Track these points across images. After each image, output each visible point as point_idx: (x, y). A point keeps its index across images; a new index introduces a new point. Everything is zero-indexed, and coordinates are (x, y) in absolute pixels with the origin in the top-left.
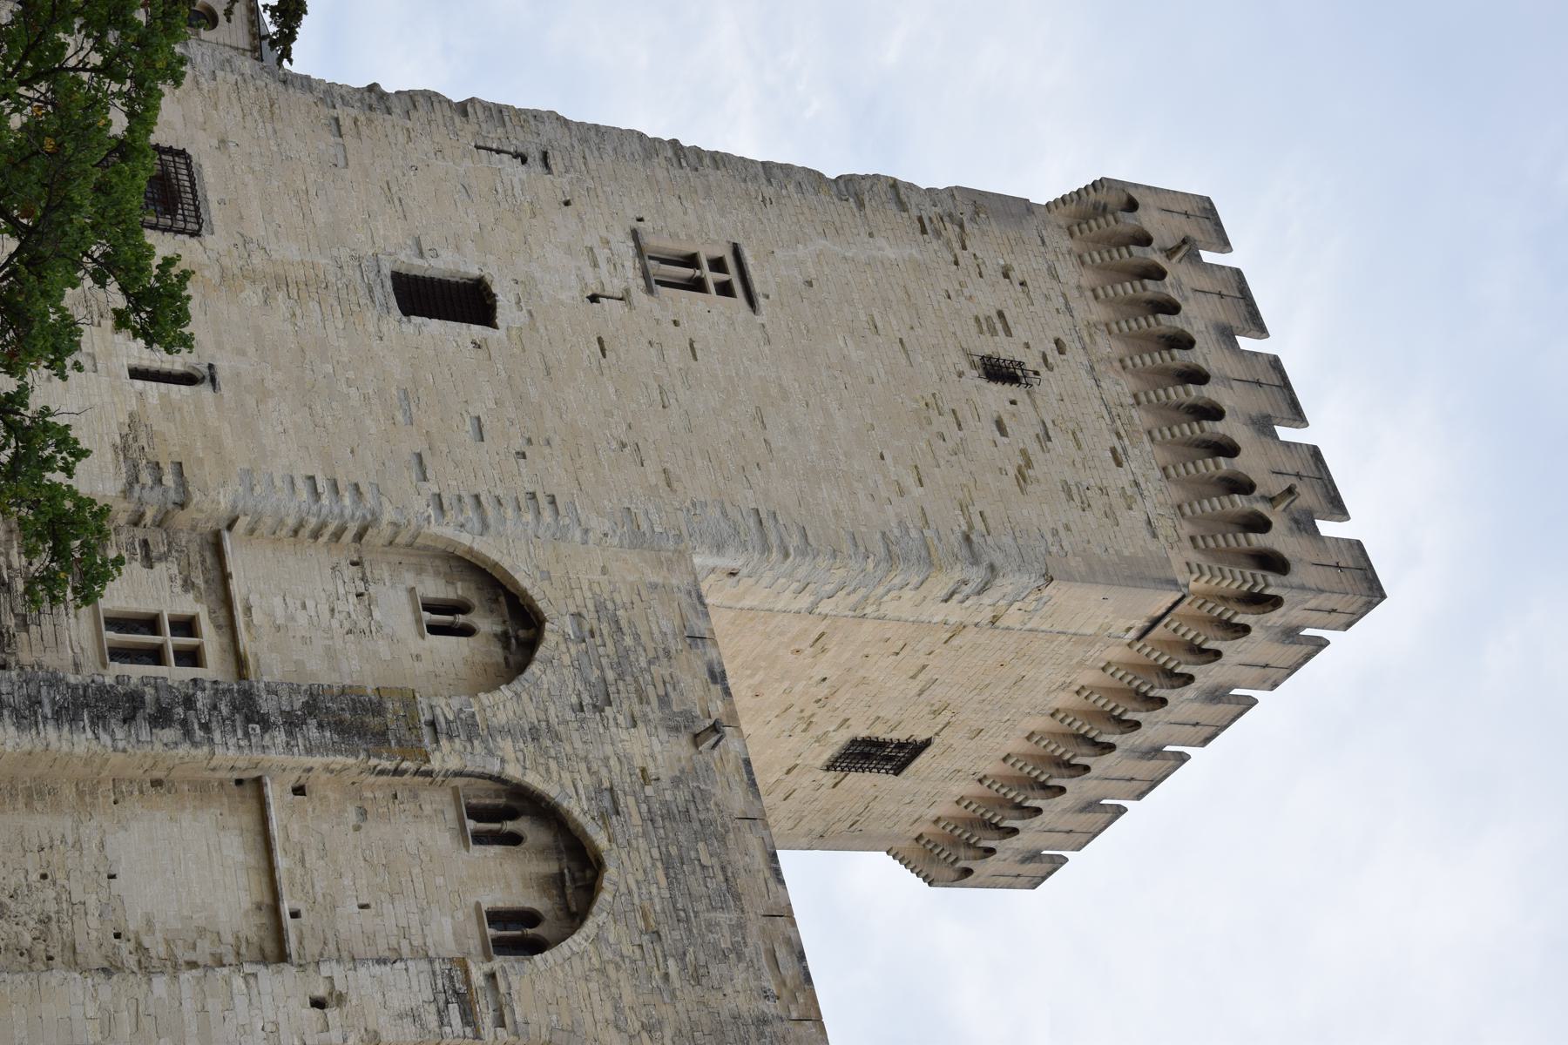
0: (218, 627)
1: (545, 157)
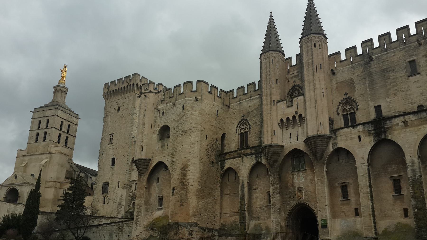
0: (136, 181)
1: (102, 152)
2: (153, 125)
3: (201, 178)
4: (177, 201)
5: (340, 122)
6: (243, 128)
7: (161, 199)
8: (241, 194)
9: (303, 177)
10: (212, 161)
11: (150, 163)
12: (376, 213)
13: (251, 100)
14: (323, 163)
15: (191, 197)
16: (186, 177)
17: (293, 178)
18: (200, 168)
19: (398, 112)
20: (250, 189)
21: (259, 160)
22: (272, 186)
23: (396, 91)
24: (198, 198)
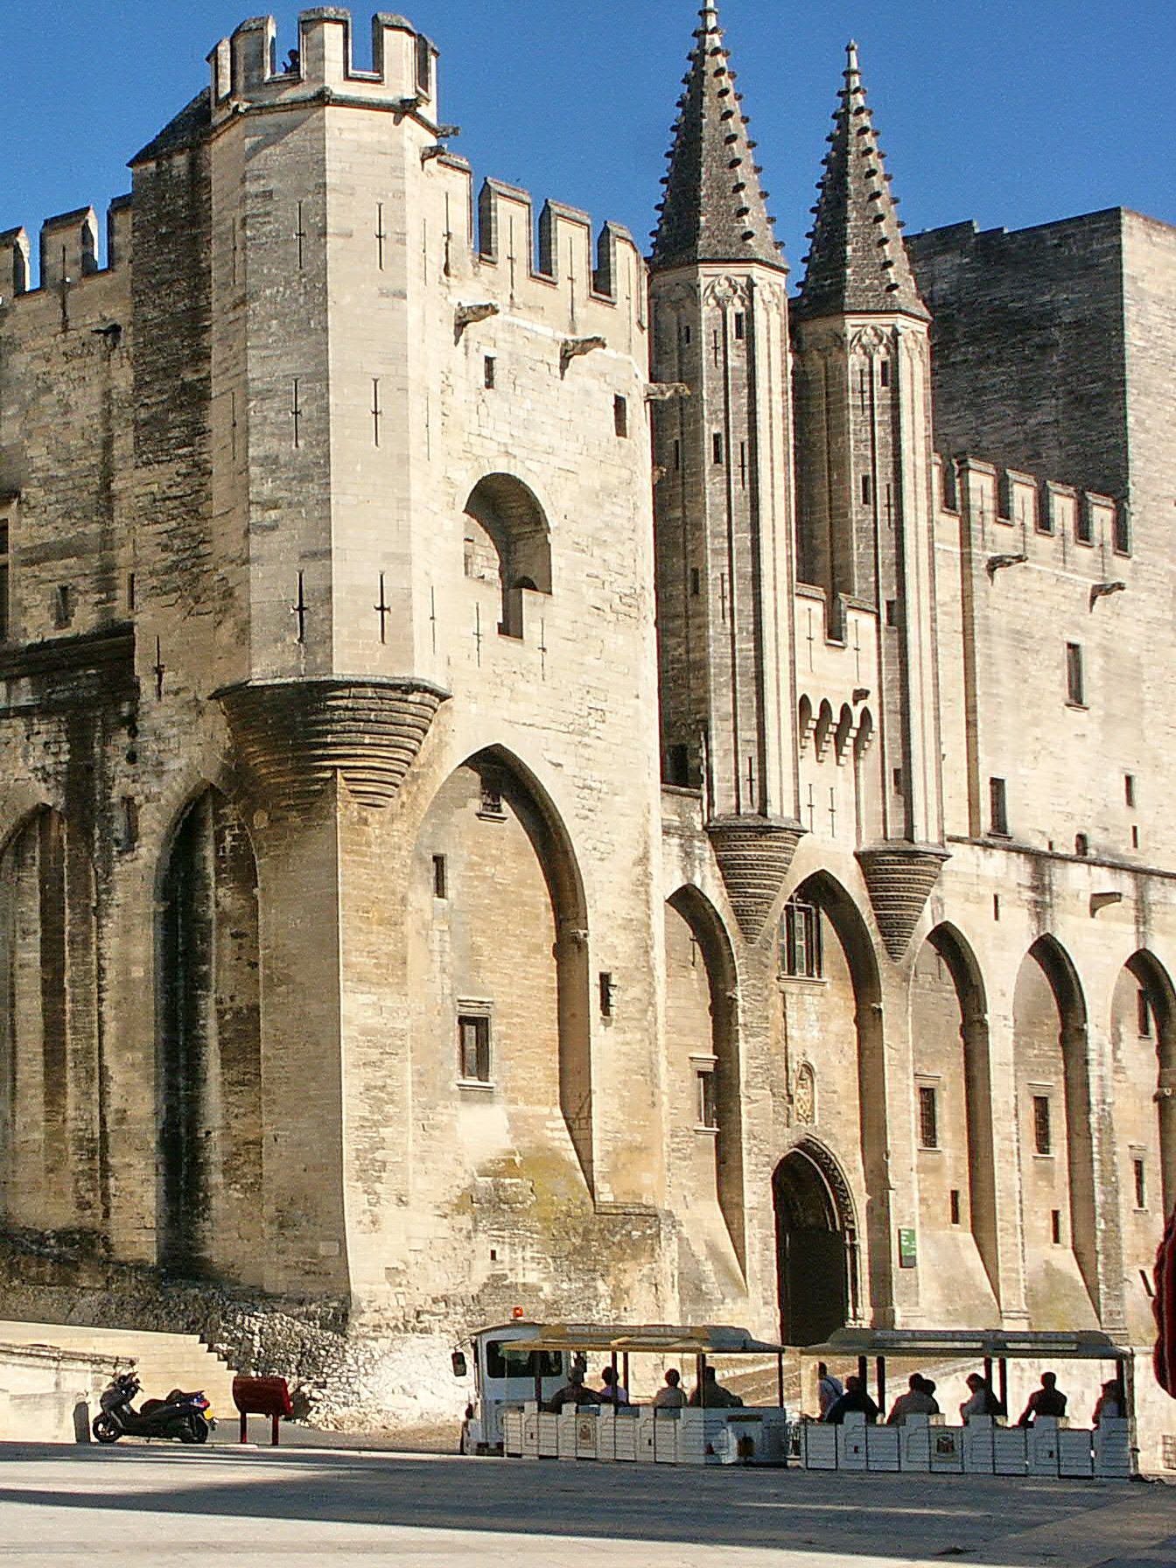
7: (475, 1026)
9: (813, 1017)
11: (431, 729)
14: (906, 980)
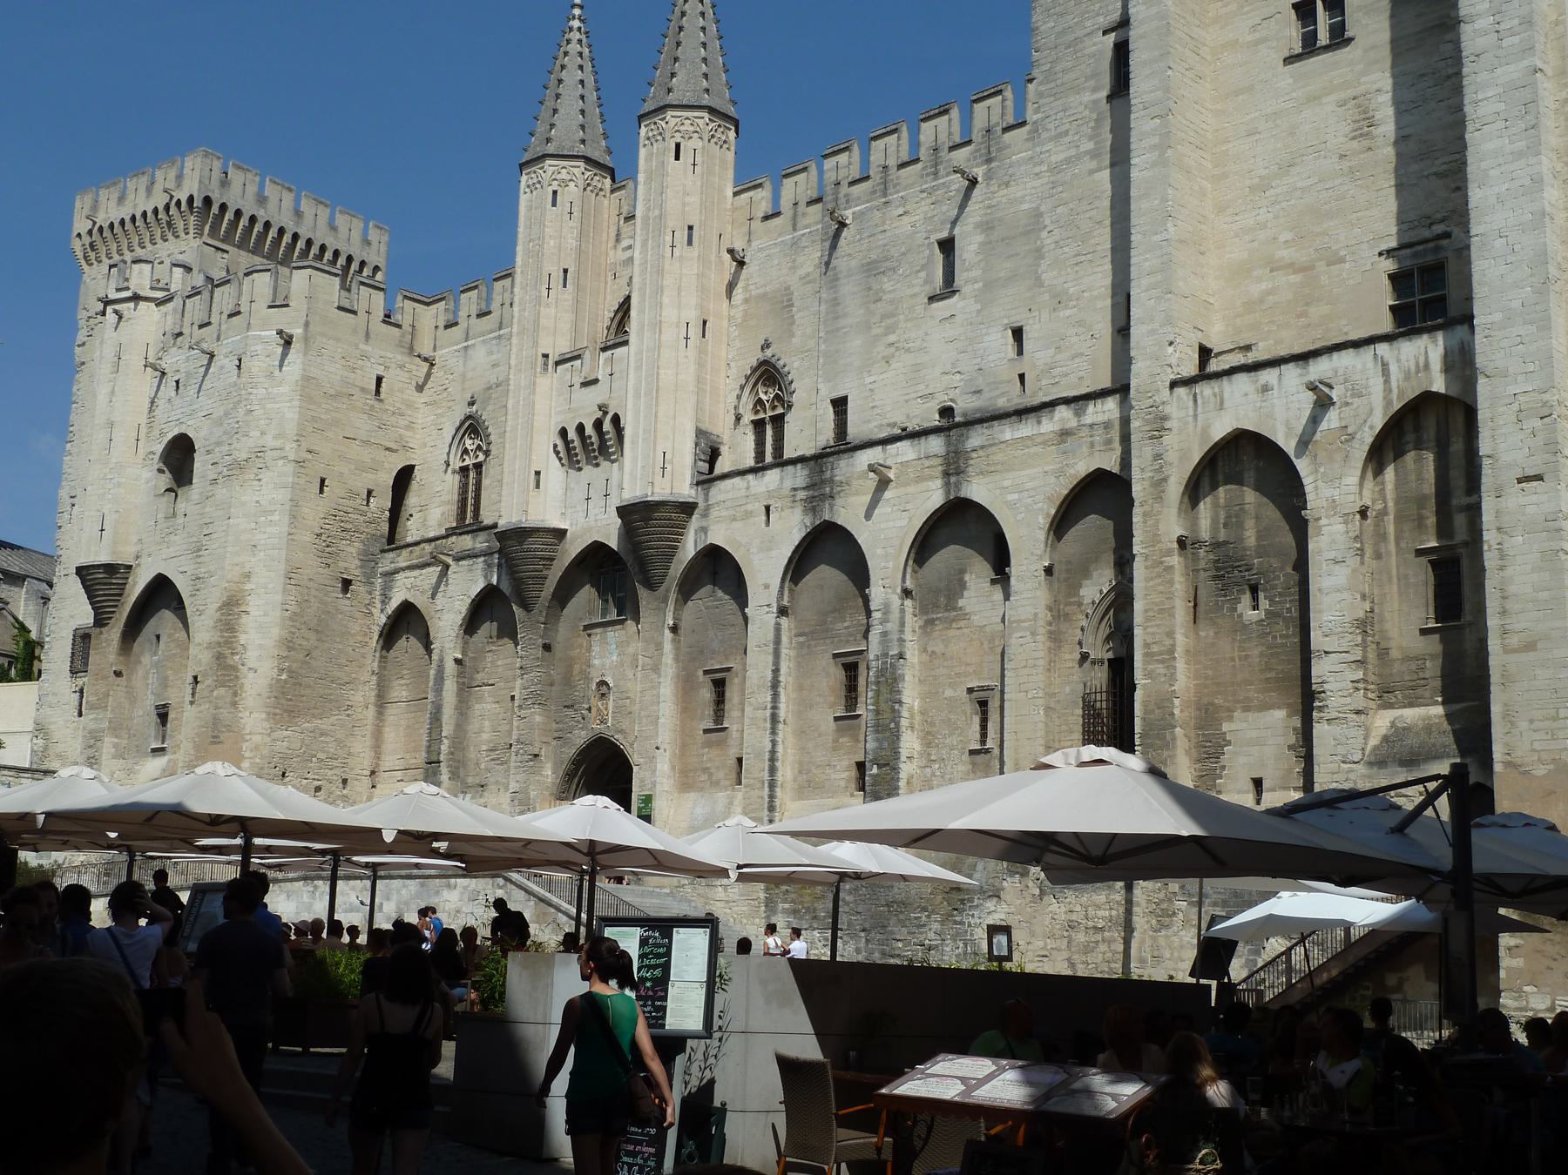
2: (143, 430)
3: (289, 644)
4: (204, 727)
5: (739, 449)
6: (469, 448)
8: (432, 702)
9: (614, 646)
10: (345, 576)
12: (779, 777)
13: (499, 337)
14: (665, 600)
15: (251, 713)
16: (235, 637)
17: (589, 649)
18: (288, 607)
19: (889, 425)
20: (466, 688)
21: (492, 577)
22: (522, 675)
23: (892, 350)
24: (271, 716)
